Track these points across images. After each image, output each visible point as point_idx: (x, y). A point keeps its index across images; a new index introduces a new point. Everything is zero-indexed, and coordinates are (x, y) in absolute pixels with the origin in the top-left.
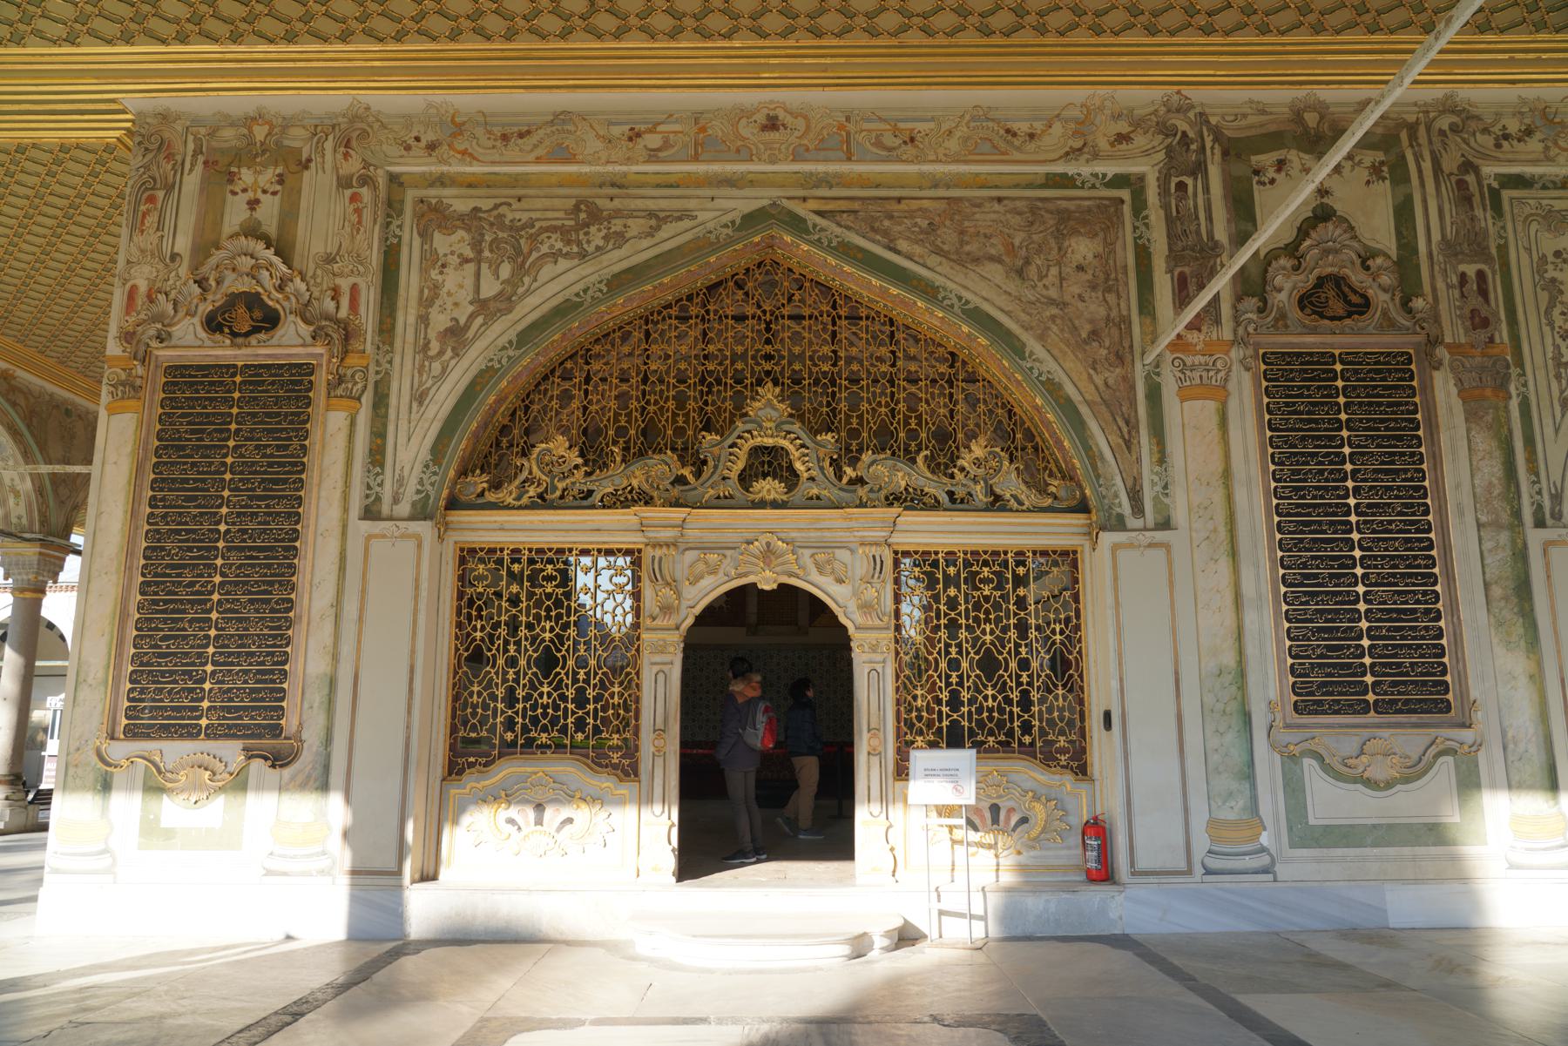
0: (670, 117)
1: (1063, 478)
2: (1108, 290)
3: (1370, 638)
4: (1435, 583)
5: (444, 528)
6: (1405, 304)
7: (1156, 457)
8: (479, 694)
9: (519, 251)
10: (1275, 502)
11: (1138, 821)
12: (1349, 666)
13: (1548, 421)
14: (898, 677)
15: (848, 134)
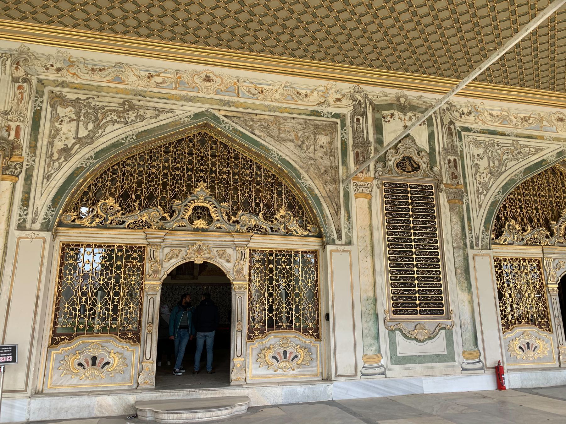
0: (166, 71)
1: (313, 224)
2: (331, 156)
3: (418, 287)
4: (439, 268)
5: (55, 236)
6: (431, 168)
7: (346, 218)
8: (68, 308)
9: (97, 119)
10: (387, 236)
11: (338, 356)
12: (411, 297)
13: (475, 212)
14: (249, 299)
15: (238, 87)
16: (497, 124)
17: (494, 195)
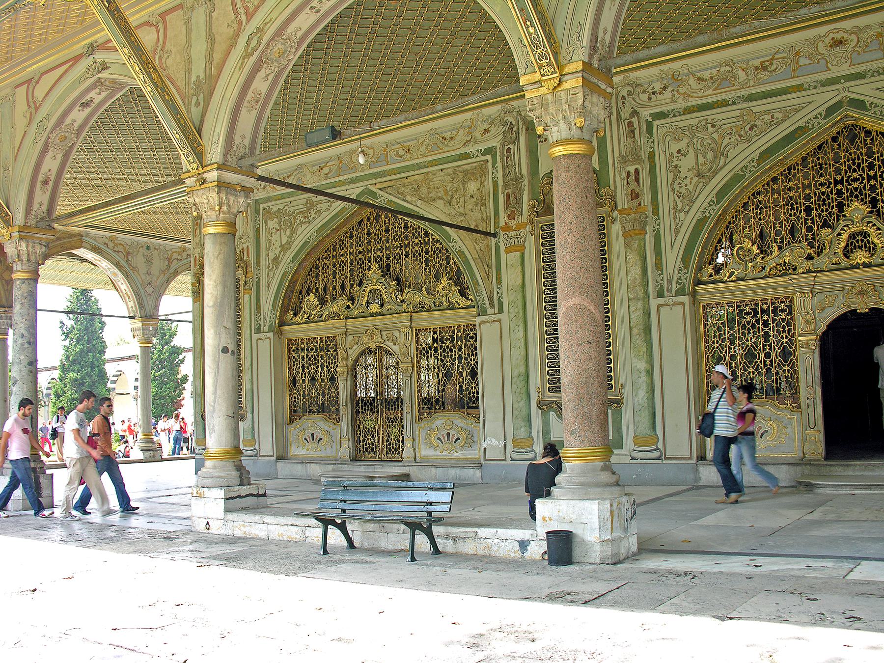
9: (291, 224)
16: (710, 92)
17: (701, 209)
